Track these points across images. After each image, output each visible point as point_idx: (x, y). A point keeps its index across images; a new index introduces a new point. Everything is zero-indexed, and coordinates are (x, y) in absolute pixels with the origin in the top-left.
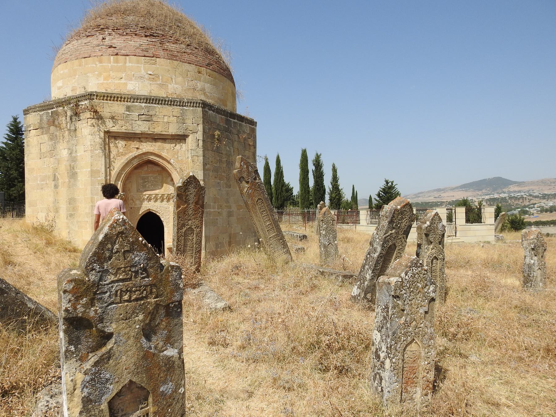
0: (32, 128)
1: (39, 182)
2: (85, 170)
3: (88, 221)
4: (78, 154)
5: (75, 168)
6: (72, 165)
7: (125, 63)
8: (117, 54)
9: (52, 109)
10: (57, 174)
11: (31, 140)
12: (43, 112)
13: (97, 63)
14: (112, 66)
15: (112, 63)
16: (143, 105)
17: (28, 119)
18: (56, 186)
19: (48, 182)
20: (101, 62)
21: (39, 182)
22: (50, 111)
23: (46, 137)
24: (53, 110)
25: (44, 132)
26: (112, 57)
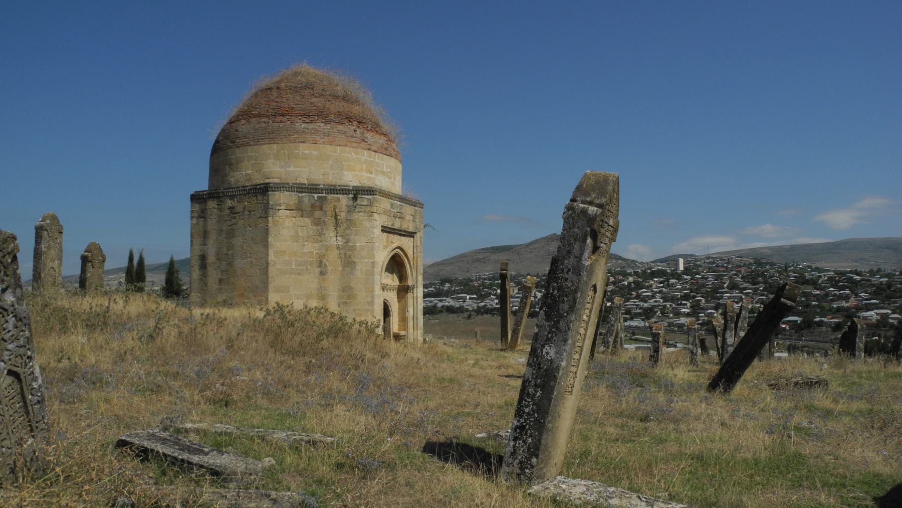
0: (282, 208)
1: (293, 267)
2: (366, 260)
3: (369, 309)
4: (358, 245)
5: (352, 257)
6: (348, 255)
7: (375, 159)
8: (369, 149)
9: (319, 193)
10: (324, 261)
11: (281, 221)
12: (304, 194)
13: (353, 154)
14: (365, 159)
15: (365, 157)
16: (399, 203)
17: (277, 197)
18: (322, 273)
19: (309, 267)
20: (356, 153)
21: (293, 267)
22: (316, 195)
23: (307, 221)
24: (320, 195)
25: (305, 215)
26: (365, 152)
